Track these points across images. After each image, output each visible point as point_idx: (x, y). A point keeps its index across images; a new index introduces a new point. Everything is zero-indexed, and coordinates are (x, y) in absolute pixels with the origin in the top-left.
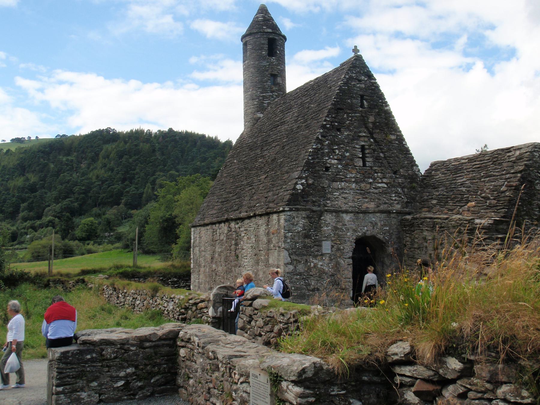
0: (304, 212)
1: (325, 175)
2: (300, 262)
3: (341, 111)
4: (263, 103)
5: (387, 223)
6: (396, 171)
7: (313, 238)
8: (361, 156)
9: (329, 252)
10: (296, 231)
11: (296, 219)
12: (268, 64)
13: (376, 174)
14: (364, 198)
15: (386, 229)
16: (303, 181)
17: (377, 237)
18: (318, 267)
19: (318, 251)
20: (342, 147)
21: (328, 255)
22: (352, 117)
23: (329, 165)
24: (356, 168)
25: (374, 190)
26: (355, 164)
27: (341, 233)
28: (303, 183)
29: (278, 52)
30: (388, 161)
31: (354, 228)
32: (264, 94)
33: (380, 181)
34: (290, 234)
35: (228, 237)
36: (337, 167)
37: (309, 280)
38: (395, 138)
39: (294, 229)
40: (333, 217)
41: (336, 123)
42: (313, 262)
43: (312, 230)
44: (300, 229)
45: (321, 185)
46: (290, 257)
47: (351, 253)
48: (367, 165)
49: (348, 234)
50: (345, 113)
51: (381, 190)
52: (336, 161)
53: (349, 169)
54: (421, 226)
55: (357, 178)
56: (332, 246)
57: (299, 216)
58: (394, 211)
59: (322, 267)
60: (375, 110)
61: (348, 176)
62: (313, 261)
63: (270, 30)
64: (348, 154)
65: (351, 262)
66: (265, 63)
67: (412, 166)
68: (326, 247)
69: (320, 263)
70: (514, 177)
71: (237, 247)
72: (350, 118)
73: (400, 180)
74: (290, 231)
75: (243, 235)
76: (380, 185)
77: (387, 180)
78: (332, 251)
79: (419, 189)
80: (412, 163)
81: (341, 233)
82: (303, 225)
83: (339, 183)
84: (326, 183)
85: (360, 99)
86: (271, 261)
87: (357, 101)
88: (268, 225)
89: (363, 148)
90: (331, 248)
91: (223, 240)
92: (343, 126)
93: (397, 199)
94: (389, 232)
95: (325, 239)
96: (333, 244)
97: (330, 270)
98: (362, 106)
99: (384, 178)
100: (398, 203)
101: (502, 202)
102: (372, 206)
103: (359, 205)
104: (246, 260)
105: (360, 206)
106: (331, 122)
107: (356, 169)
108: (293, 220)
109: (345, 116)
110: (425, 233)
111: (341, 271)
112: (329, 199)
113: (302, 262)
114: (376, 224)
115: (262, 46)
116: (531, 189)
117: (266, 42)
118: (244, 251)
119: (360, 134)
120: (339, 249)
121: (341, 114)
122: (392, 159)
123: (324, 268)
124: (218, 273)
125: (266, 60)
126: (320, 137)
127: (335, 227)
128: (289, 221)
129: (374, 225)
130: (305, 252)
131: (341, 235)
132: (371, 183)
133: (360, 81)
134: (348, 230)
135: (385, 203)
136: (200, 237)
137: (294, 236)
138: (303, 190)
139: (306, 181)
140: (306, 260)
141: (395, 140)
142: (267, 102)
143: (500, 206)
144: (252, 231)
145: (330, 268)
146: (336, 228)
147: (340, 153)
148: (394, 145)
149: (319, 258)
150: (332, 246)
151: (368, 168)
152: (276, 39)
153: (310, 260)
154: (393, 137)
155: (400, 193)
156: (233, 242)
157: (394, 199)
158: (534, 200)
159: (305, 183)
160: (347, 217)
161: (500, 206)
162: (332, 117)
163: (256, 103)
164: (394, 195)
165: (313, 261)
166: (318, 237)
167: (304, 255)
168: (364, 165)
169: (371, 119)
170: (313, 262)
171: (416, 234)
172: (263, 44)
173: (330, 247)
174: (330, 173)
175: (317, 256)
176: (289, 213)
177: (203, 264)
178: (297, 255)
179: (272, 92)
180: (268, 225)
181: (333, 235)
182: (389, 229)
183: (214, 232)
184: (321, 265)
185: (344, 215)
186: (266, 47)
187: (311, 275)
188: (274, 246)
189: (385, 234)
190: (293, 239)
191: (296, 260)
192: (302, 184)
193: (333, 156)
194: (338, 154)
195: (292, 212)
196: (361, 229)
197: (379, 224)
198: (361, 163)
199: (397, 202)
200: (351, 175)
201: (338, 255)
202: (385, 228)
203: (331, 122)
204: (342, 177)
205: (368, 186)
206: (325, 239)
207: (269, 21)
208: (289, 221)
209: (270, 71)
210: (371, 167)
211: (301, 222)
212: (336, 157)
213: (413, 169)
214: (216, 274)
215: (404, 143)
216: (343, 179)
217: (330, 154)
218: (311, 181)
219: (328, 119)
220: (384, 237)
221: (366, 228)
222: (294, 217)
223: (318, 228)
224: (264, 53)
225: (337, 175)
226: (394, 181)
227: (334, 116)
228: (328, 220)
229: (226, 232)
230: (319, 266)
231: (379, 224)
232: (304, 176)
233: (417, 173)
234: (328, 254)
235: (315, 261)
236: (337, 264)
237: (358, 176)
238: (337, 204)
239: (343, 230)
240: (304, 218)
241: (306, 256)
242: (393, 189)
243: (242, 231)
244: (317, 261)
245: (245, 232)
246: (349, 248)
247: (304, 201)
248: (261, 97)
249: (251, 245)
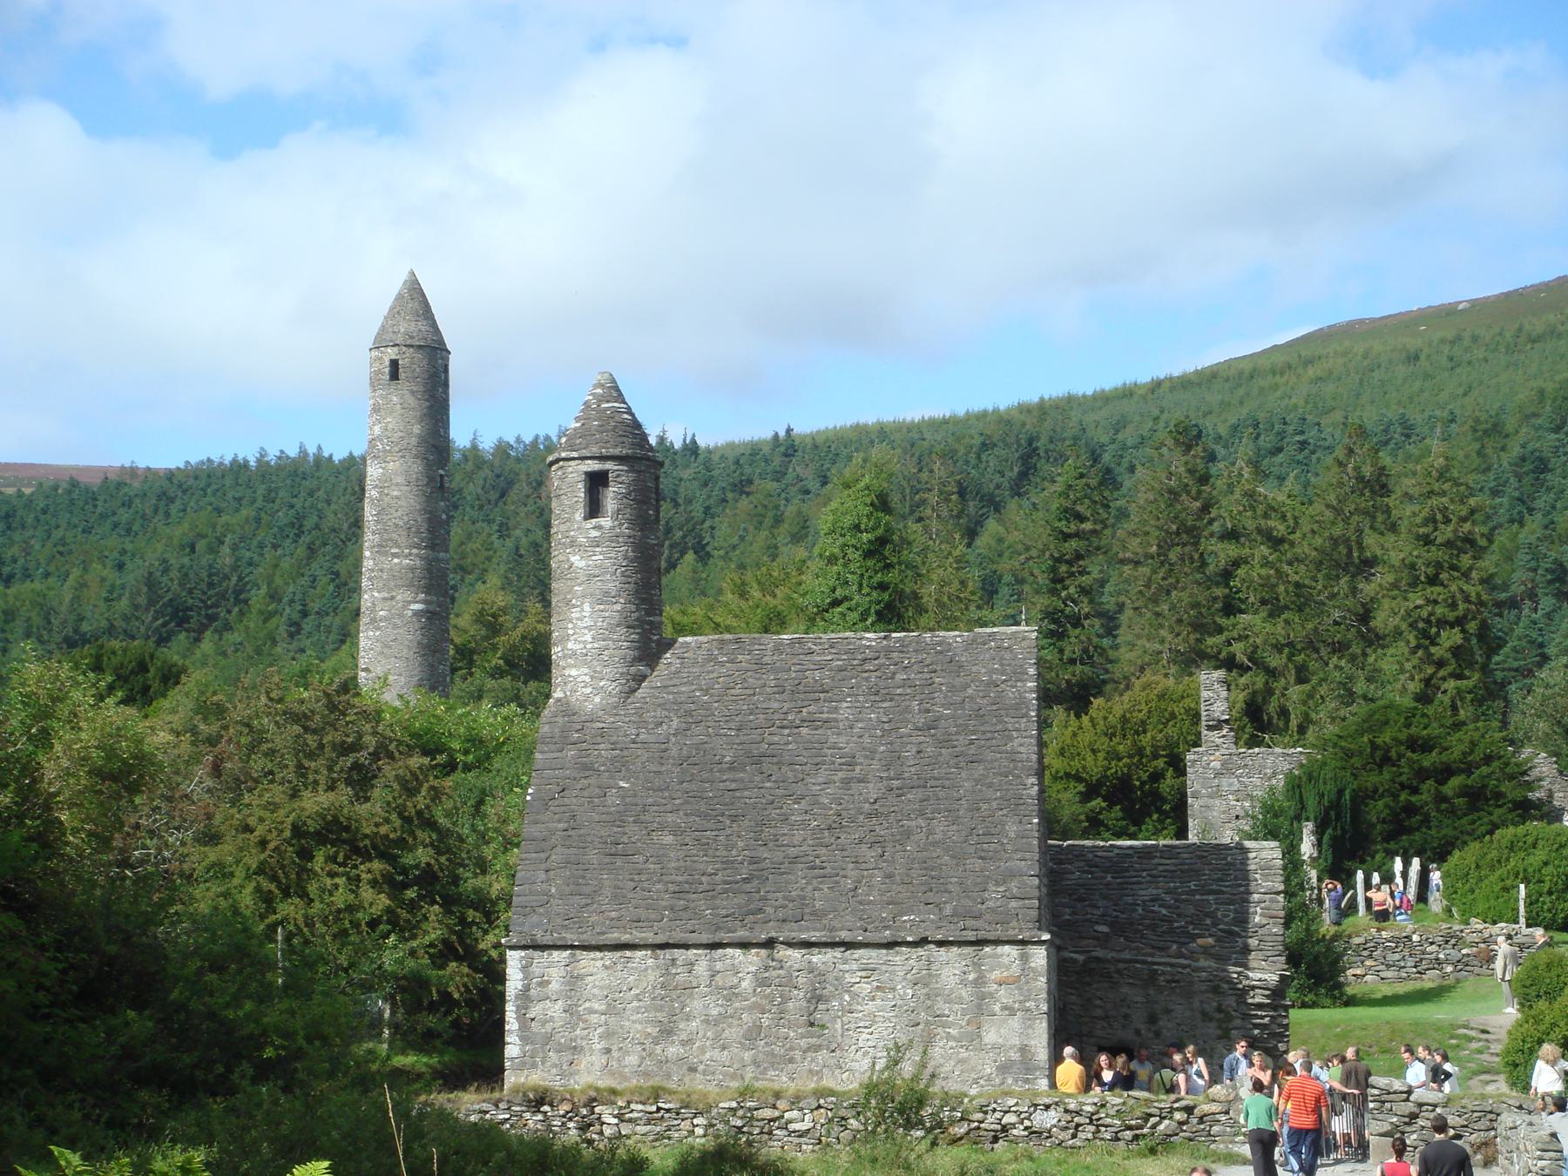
35: (762, 982)
86: (990, 1036)
88: (977, 965)
124: (701, 1067)
171: (1097, 990)
188: (1005, 1008)
245: (859, 974)
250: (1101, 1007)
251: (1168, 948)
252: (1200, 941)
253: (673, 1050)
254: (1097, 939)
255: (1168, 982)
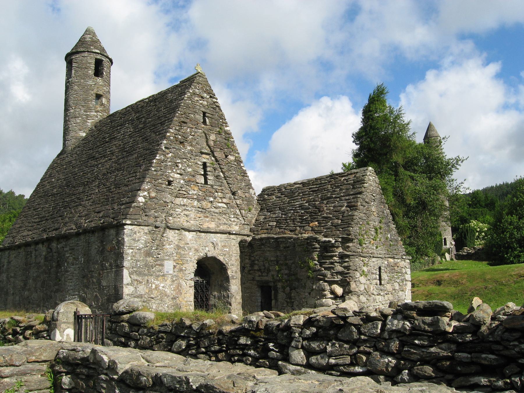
0: (146, 228)
1: (168, 189)
2: (141, 283)
3: (185, 125)
4: (87, 122)
5: (227, 244)
6: (235, 192)
7: (155, 257)
8: (203, 173)
9: (171, 272)
10: (138, 248)
11: (138, 234)
12: (94, 83)
13: (216, 193)
14: (205, 217)
15: (227, 251)
16: (146, 193)
17: (218, 258)
18: (159, 289)
19: (160, 271)
20: (185, 162)
21: (170, 276)
22: (195, 132)
23: (171, 179)
24: (198, 184)
25: (215, 209)
26: (197, 181)
27: (183, 252)
28: (145, 195)
29: (105, 74)
30: (227, 181)
31: (196, 247)
32: (88, 113)
33: (220, 201)
34: (131, 251)
36: (179, 182)
37: (150, 303)
38: (234, 158)
39: (136, 245)
40: (176, 235)
41: (180, 135)
42: (154, 283)
43: (154, 248)
44: (141, 246)
45: (164, 199)
46: (131, 277)
47: (193, 274)
48: (208, 183)
49: (191, 254)
50: (189, 127)
51: (221, 210)
52: (179, 175)
53: (191, 185)
54: (263, 247)
55: (199, 195)
56: (174, 266)
57: (141, 231)
58: (234, 232)
59: (164, 289)
60: (216, 128)
61: (190, 193)
62: (155, 281)
63: (98, 51)
64: (190, 170)
65: (193, 284)
66: (90, 82)
67: (249, 188)
68: (169, 266)
69: (162, 285)
70: (353, 198)
71: (60, 270)
72: (193, 133)
73: (238, 201)
74: (132, 248)
75: (68, 255)
76: (220, 205)
77: (226, 200)
78: (174, 272)
79: (255, 212)
80: (249, 186)
81: (183, 252)
82: (145, 241)
83: (181, 199)
84: (169, 198)
85: (202, 115)
86: (104, 283)
87: (200, 118)
89: (205, 165)
90: (174, 268)
91: (40, 263)
92: (186, 140)
93: (236, 220)
94: (229, 253)
95: (168, 257)
96: (175, 264)
97: (172, 292)
98: (204, 122)
99: (224, 198)
100: (236, 225)
101: (345, 221)
102: (212, 226)
103: (200, 224)
104: (71, 284)
105: (201, 225)
106: (175, 134)
107: (198, 186)
108: (135, 235)
109: (188, 130)
110: (268, 254)
111: (183, 294)
112: (171, 215)
113: (143, 283)
114: (217, 244)
115: (88, 65)
116: (368, 210)
117: (93, 61)
118: (68, 273)
119: (203, 151)
120: (181, 270)
121: (185, 128)
122: (231, 179)
123: (166, 290)
124: (31, 301)
125: (92, 79)
126: (164, 148)
127: (177, 245)
128: (130, 236)
129: (214, 245)
130: (146, 272)
131: (183, 255)
132: (211, 202)
133: (202, 97)
134: (190, 249)
135: (225, 224)
136: (9, 262)
137: (136, 253)
138: (145, 204)
139: (149, 193)
140: (148, 280)
141: (235, 161)
142: (90, 121)
143: (344, 225)
144: (80, 250)
145: (172, 290)
146: (178, 247)
147: (183, 168)
148: (233, 165)
149: (160, 278)
150: (175, 267)
151: (209, 186)
152: (103, 60)
153: (151, 281)
154: (231, 158)
155: (238, 215)
156: (54, 264)
157: (233, 220)
158: (370, 221)
159: (147, 195)
160: (189, 236)
161: (344, 225)
162: (175, 129)
163: (78, 121)
164: (232, 216)
165: (155, 281)
166: (159, 256)
167: (145, 275)
168: (206, 182)
169: (212, 137)
170: (155, 283)
172: (90, 63)
173: (172, 267)
174: (173, 188)
175: (158, 276)
176: (130, 227)
177: (12, 292)
178: (138, 275)
179: (97, 112)
180: (102, 242)
181: (175, 254)
182: (229, 250)
183: (28, 255)
184: (163, 287)
185: (187, 233)
186: (93, 66)
187: (152, 298)
189: (225, 255)
190: (134, 256)
191: (137, 280)
192: (144, 197)
193: (176, 170)
194: (181, 169)
195: (134, 226)
196: (203, 249)
197: (220, 245)
198: (203, 181)
199: (235, 223)
200: (193, 192)
201: (180, 276)
202: (225, 249)
203: (175, 134)
204: (184, 193)
205: (209, 205)
206: (168, 257)
207: (97, 43)
208: (130, 236)
209: (95, 91)
210: (212, 186)
211: (143, 238)
212: (178, 172)
213: (249, 192)
214: (29, 302)
215: (242, 165)
216: (185, 195)
217: (173, 168)
218: (153, 194)
219: (172, 131)
220: (224, 259)
221: (207, 249)
222: (136, 232)
223: (160, 246)
224: (90, 72)
225: (179, 190)
226: (233, 202)
227: (177, 128)
228: (171, 237)
229: (44, 253)
230: (161, 288)
231: (220, 245)
232: (146, 188)
233: (253, 196)
234: (170, 274)
235: (157, 282)
236: (179, 285)
237: (200, 194)
238: (179, 221)
239: (185, 249)
240: (146, 233)
241: (148, 276)
242: (232, 210)
243: (66, 251)
244: (159, 282)
245: (70, 252)
246: (191, 267)
247: (146, 215)
248: (85, 115)
249: (78, 266)
250: (258, 265)
251: (296, 230)
252: (311, 225)
253: (26, 293)
254: (267, 229)
255: (285, 248)
